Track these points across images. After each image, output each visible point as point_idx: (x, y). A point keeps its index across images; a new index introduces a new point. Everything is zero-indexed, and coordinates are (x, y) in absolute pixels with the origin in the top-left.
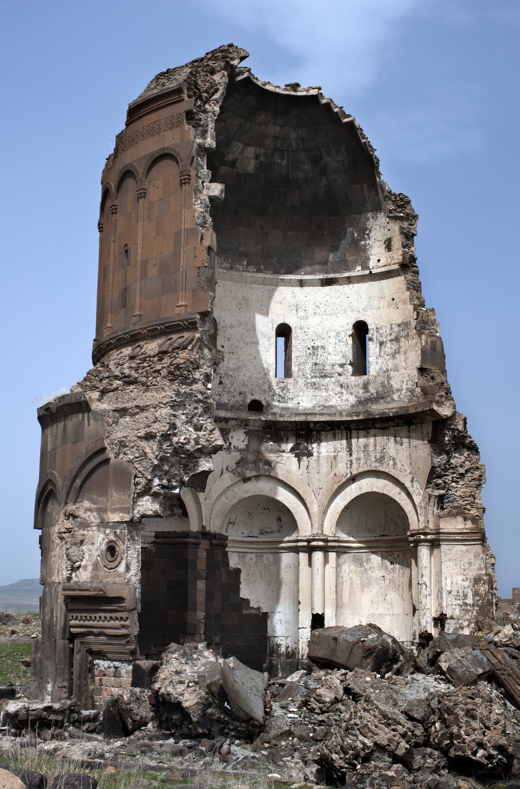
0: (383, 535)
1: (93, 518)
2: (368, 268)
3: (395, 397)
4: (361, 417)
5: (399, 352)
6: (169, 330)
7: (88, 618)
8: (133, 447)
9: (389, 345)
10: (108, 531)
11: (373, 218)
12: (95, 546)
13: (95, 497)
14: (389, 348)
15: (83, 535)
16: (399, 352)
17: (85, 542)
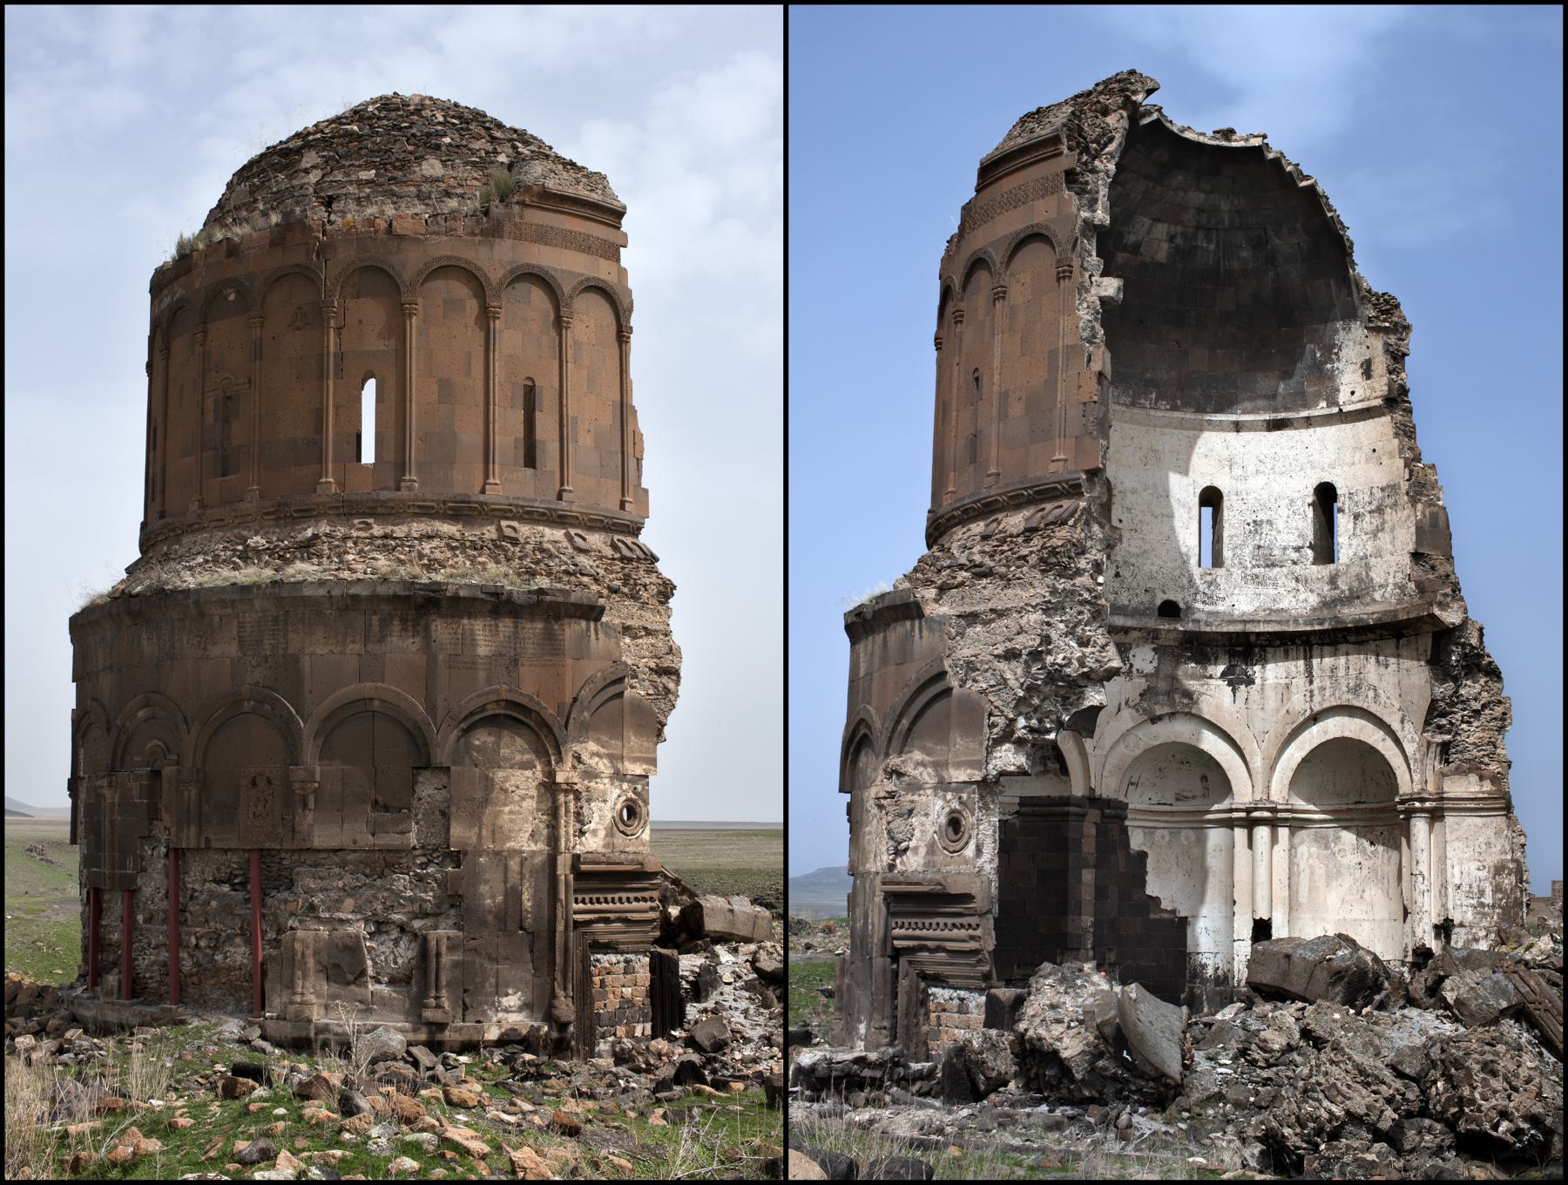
1: (927, 776)
2: (1337, 404)
3: (1377, 596)
4: (1326, 626)
9: (1367, 518)
10: (949, 796)
13: (930, 745)
14: (1368, 522)
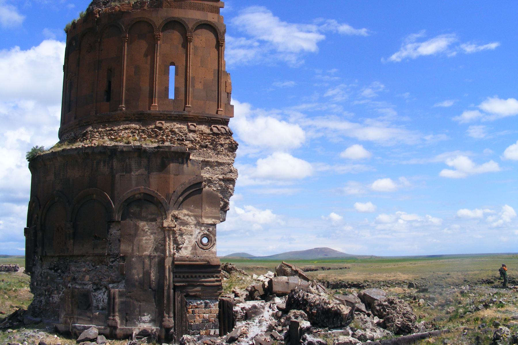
1: (191, 220)
10: (203, 228)
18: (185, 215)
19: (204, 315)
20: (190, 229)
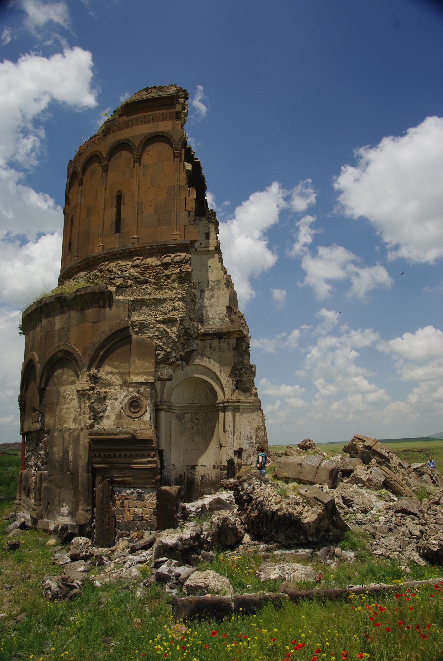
0: (192, 403)
1: (116, 379)
2: (194, 248)
3: (211, 322)
5: (213, 297)
6: (166, 250)
7: (112, 456)
8: (153, 328)
10: (131, 389)
11: (198, 220)
12: (118, 401)
13: (117, 364)
15: (106, 392)
16: (213, 297)
17: (107, 398)
18: (108, 373)
19: (136, 509)
20: (113, 391)
